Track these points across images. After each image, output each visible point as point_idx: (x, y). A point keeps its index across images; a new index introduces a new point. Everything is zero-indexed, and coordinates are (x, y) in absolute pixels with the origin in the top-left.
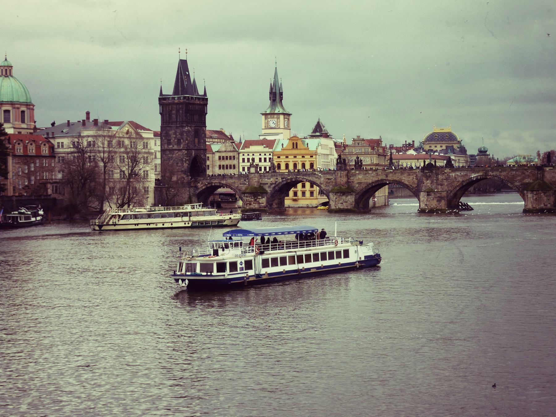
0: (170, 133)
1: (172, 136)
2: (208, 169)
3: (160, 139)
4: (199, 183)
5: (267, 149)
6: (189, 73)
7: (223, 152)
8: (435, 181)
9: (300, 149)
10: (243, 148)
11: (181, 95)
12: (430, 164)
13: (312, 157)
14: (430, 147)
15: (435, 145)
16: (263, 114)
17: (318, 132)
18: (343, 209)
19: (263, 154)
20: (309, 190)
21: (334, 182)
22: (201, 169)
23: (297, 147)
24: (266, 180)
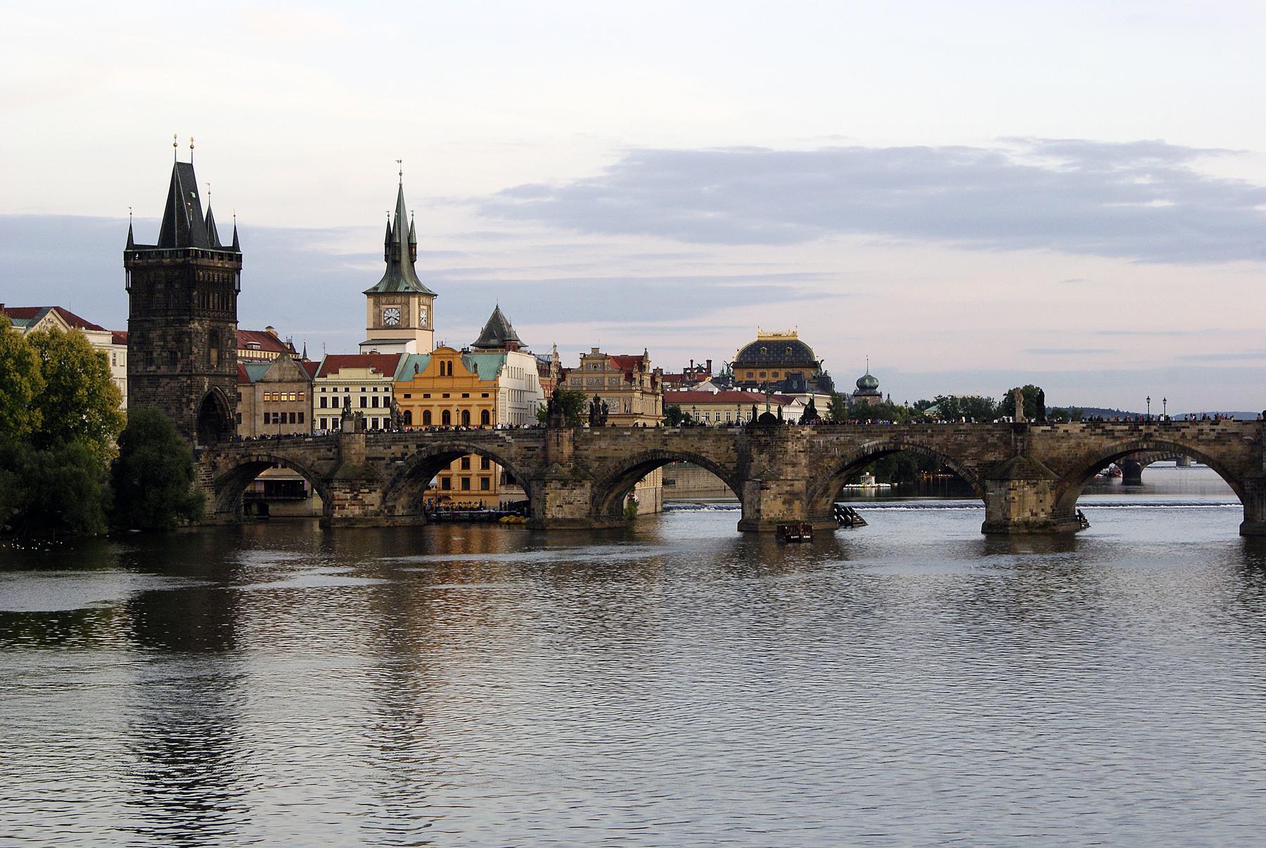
0: (151, 335)
1: (155, 344)
3: (126, 351)
4: (219, 455)
5: (381, 377)
7: (275, 382)
10: (323, 375)
11: (179, 246)
12: (767, 415)
13: (485, 395)
14: (750, 375)
15: (762, 370)
17: (494, 337)
18: (564, 519)
19: (369, 389)
20: (478, 475)
21: (542, 455)
22: (224, 422)
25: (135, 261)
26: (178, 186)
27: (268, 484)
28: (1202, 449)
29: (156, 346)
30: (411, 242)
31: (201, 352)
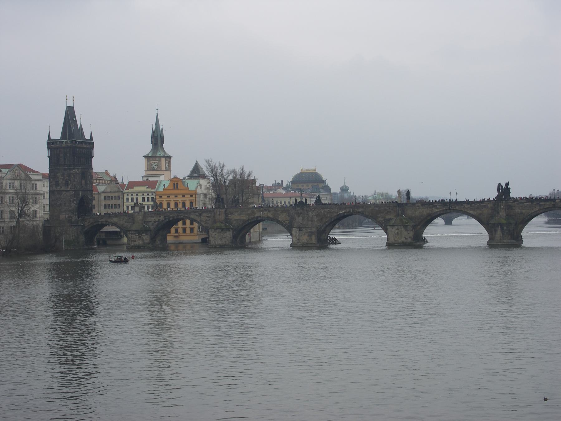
0: (58, 175)
1: (60, 178)
2: (95, 208)
3: (48, 181)
4: (86, 221)
5: (150, 190)
6: (76, 119)
8: (306, 218)
9: (181, 189)
10: (127, 189)
11: (69, 139)
12: (301, 202)
13: (191, 196)
15: (302, 184)
16: (145, 157)
17: (196, 173)
19: (146, 194)
20: (189, 227)
23: (177, 187)
24: (149, 219)
25: (51, 146)
26: (68, 116)
27: (107, 233)
28: (471, 212)
29: (61, 179)
30: (161, 136)
31: (78, 181)
